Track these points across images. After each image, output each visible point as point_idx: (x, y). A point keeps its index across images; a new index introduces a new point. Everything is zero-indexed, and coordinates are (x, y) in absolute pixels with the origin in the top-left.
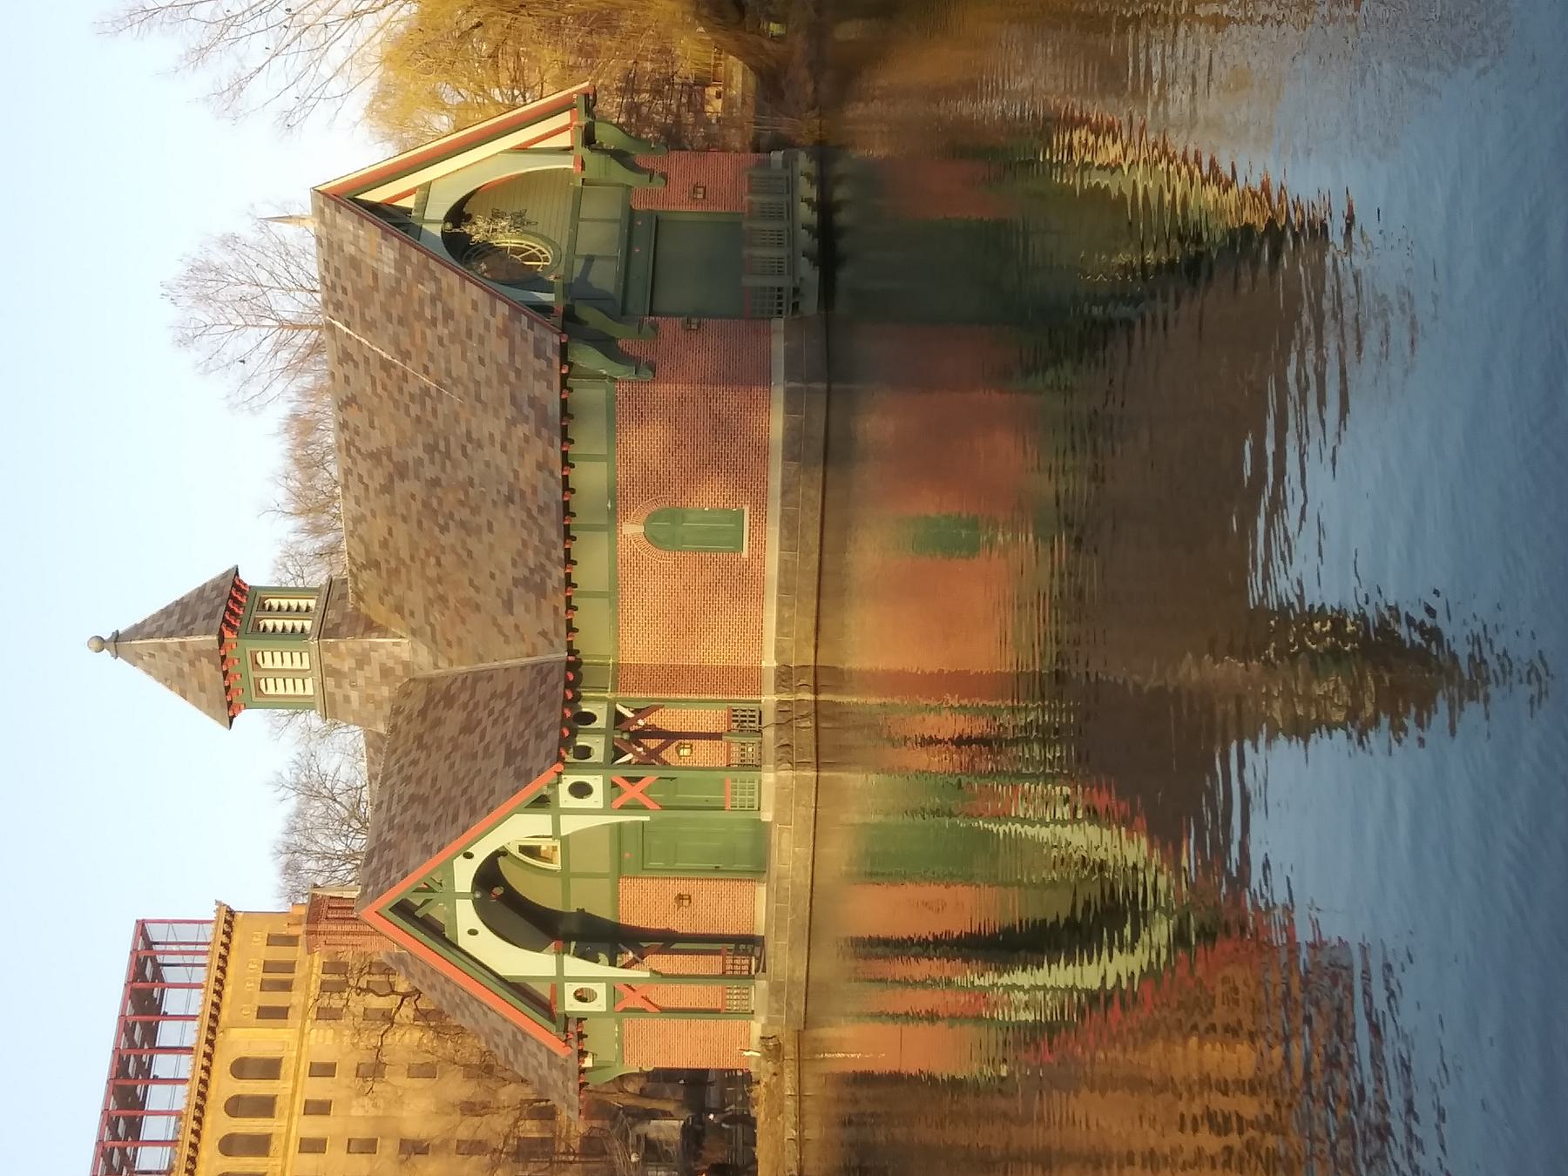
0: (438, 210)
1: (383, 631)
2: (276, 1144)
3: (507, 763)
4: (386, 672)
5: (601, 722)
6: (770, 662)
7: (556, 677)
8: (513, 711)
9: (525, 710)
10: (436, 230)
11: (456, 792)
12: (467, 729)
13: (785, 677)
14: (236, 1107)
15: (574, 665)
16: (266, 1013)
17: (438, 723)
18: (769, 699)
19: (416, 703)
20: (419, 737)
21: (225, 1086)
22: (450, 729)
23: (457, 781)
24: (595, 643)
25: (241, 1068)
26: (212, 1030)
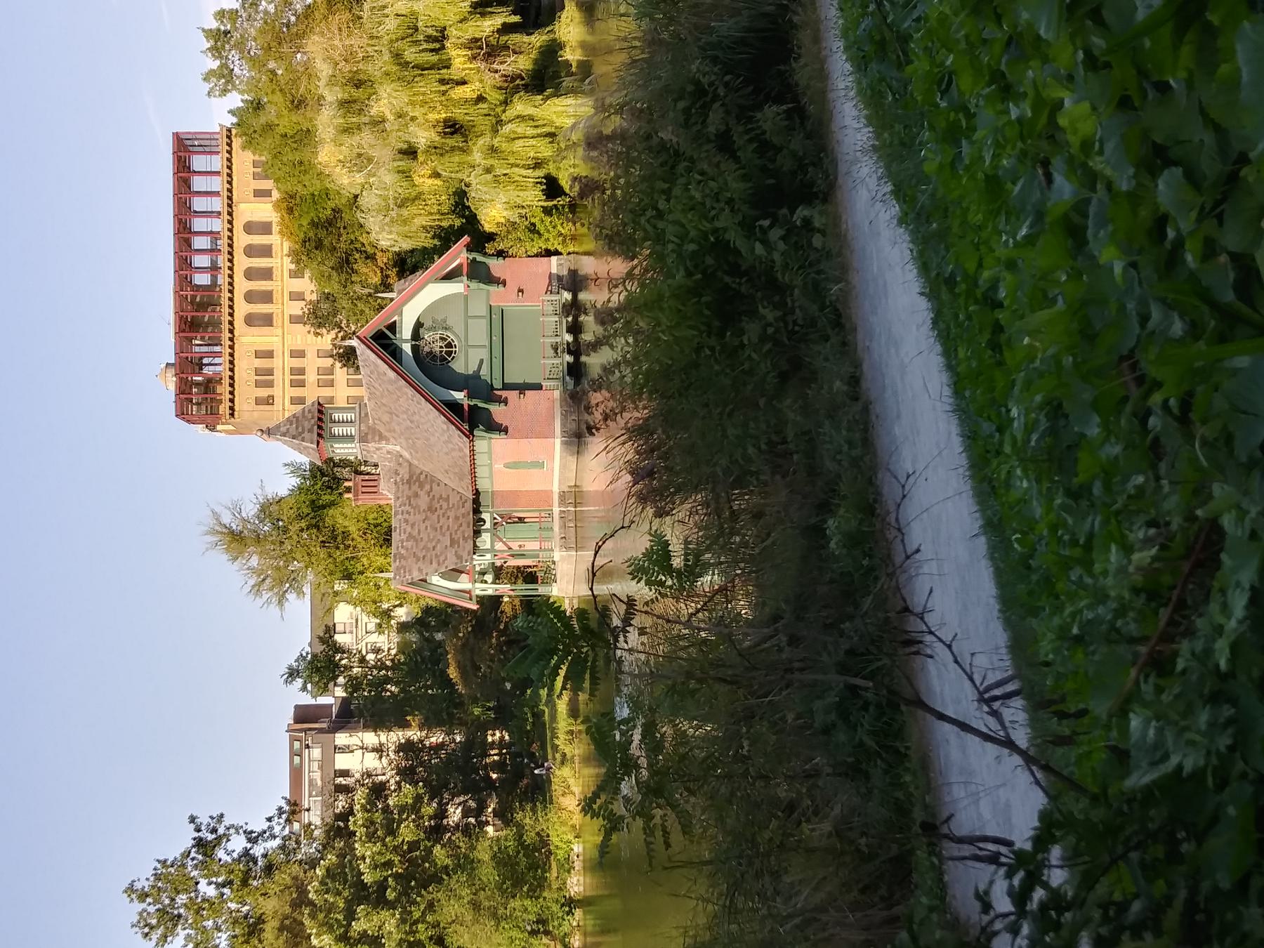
0: (406, 332)
1: (387, 440)
2: (276, 273)
3: (453, 542)
4: (388, 452)
5: (488, 525)
6: (556, 489)
7: (469, 505)
8: (451, 514)
9: (457, 518)
10: (407, 348)
11: (430, 545)
12: (431, 509)
13: (563, 496)
14: (250, 251)
15: (476, 502)
16: (259, 194)
17: (416, 495)
18: (556, 510)
19: (404, 472)
20: (409, 498)
21: (242, 240)
22: (423, 501)
23: (430, 541)
24: (483, 485)
25: (250, 228)
26: (230, 206)
